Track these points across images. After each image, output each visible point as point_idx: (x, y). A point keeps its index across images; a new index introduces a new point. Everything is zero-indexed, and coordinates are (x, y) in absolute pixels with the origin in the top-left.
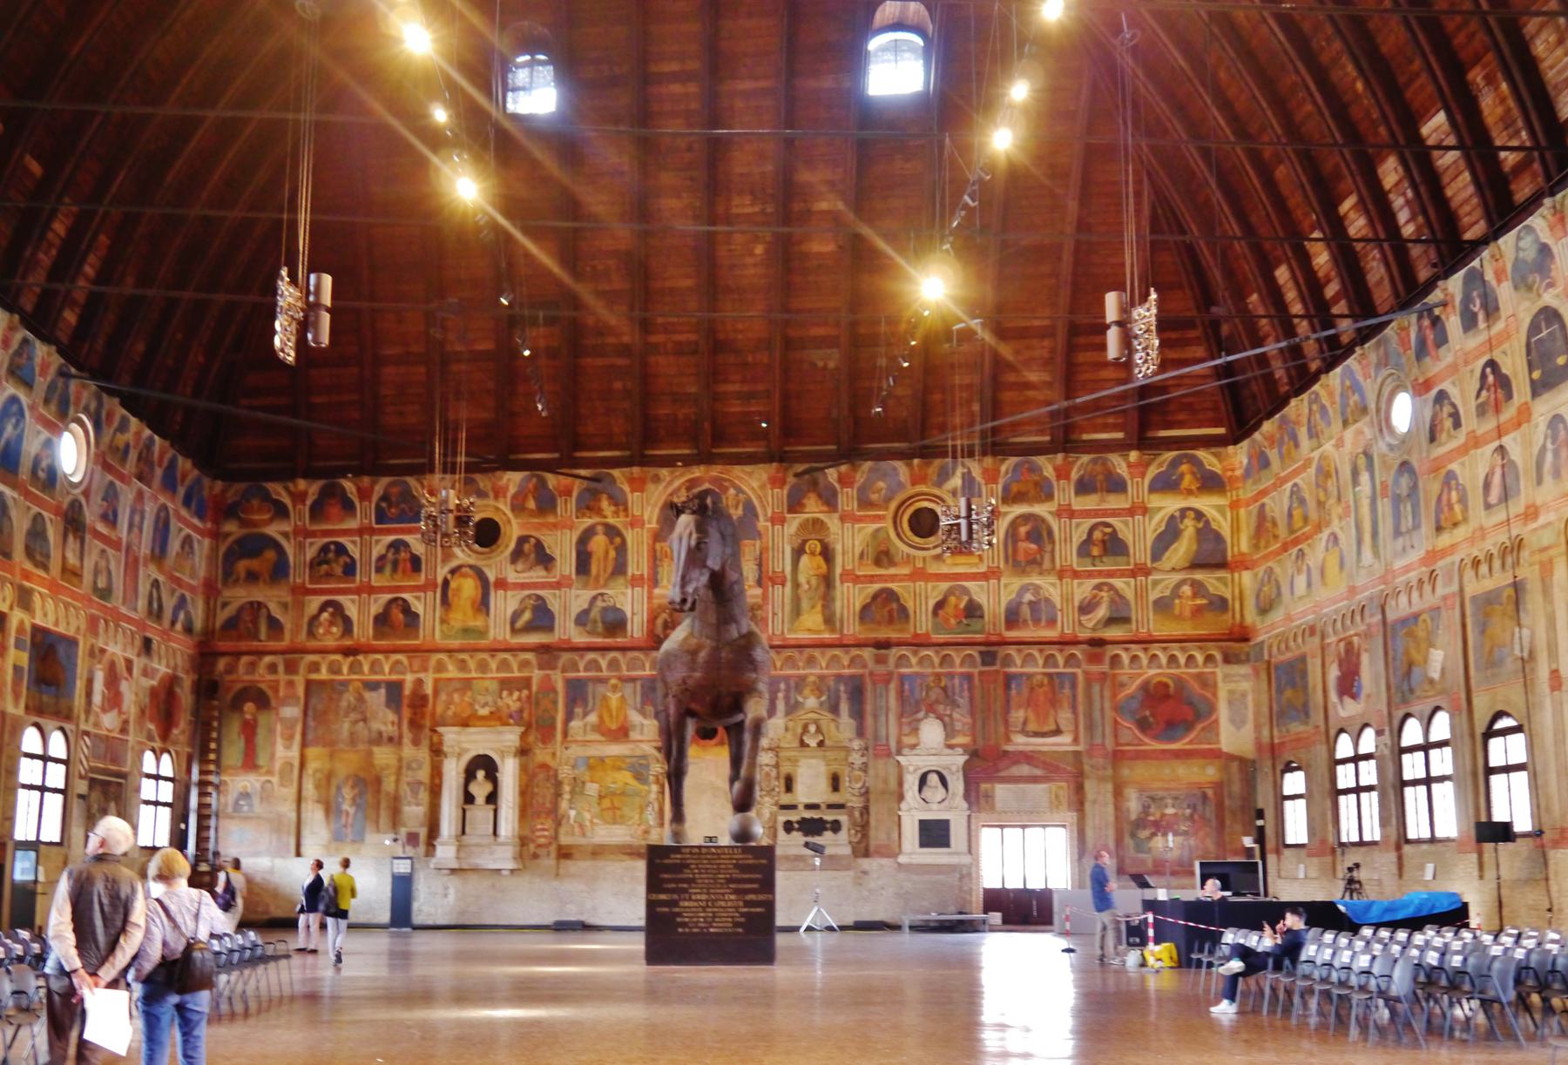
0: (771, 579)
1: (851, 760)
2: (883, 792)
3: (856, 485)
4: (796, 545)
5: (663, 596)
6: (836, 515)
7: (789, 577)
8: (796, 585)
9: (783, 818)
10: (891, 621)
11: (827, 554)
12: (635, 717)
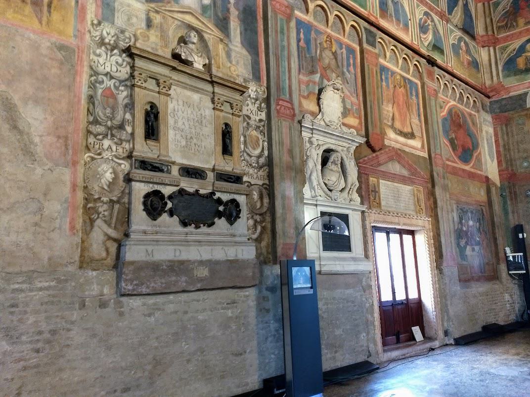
9: (140, 189)
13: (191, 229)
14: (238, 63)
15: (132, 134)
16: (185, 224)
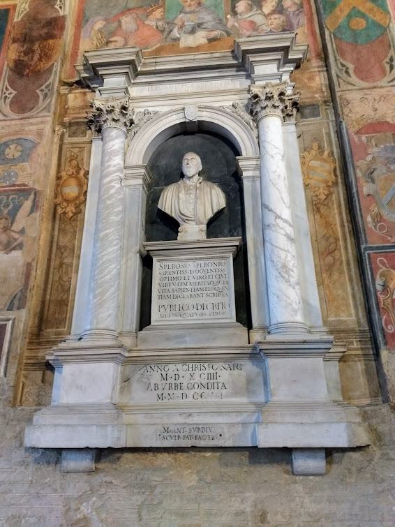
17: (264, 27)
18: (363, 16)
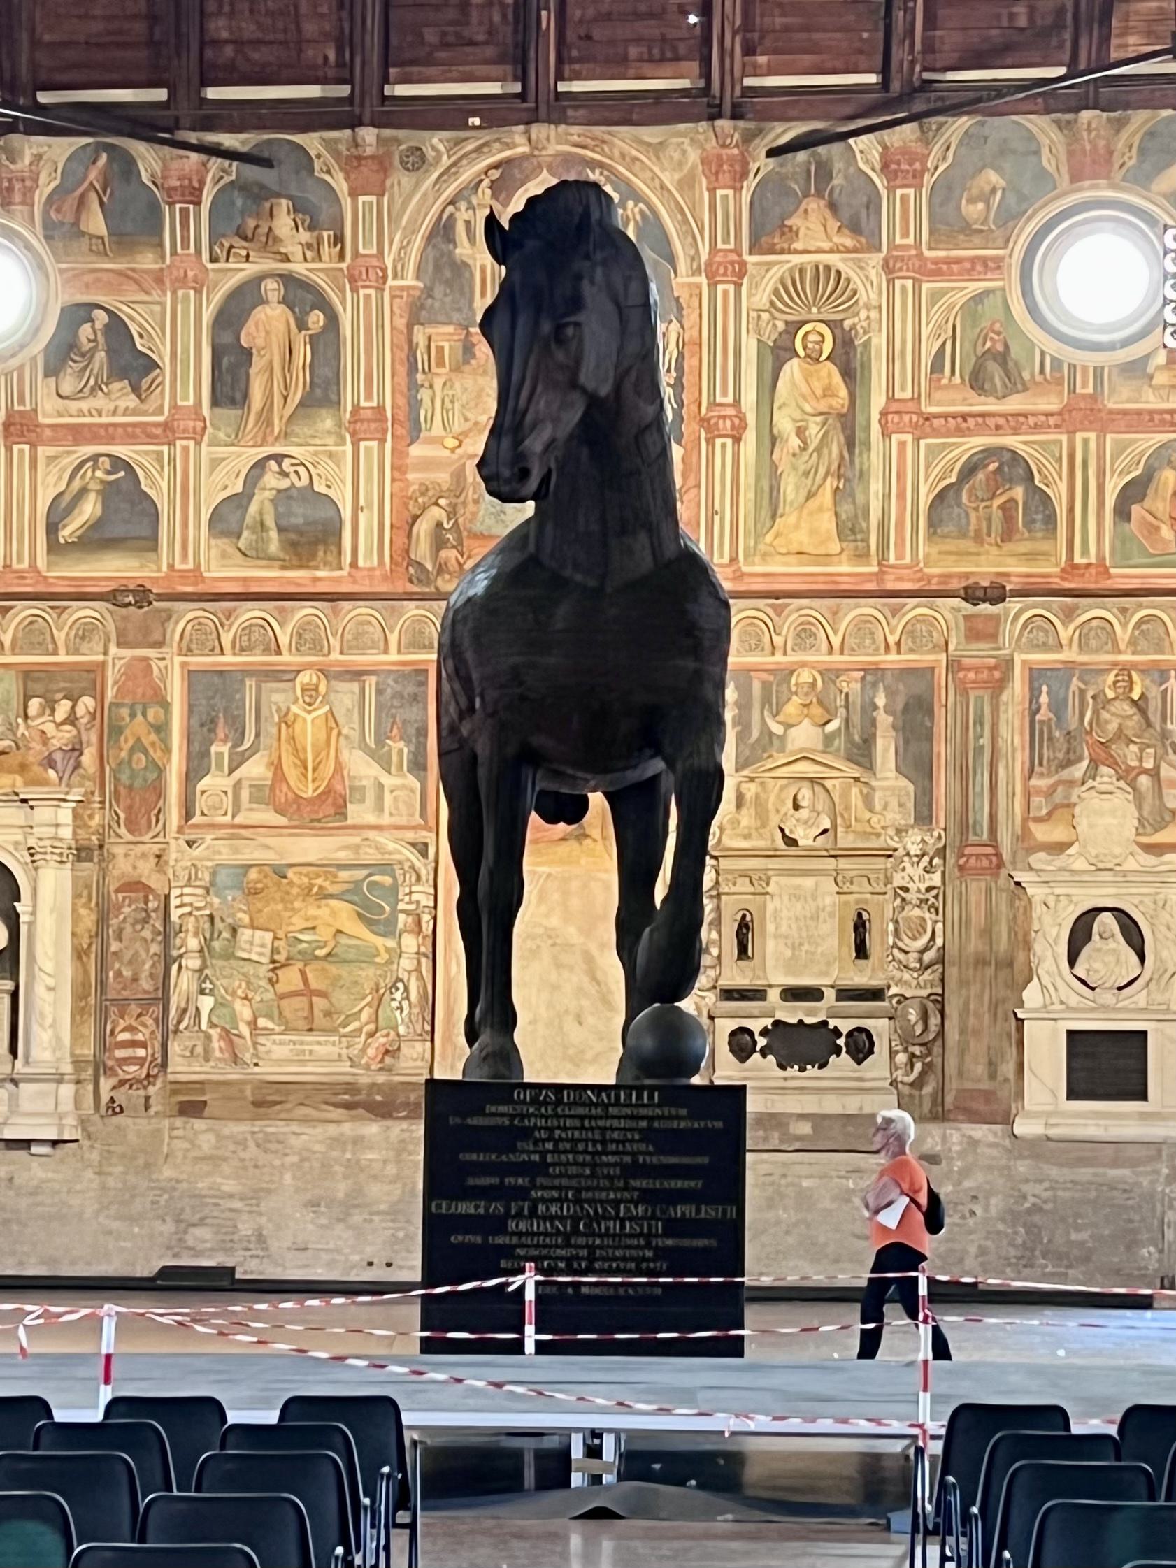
0: (704, 422)
1: (898, 880)
2: (981, 961)
3: (928, 180)
4: (770, 338)
5: (427, 464)
6: (876, 259)
7: (751, 419)
8: (772, 440)
9: (726, 1026)
10: (1008, 534)
11: (848, 359)
12: (362, 768)
13: (793, 1071)
14: (885, 807)
15: (719, 957)
16: (782, 1067)
17: (54, 741)
18: (146, 753)
